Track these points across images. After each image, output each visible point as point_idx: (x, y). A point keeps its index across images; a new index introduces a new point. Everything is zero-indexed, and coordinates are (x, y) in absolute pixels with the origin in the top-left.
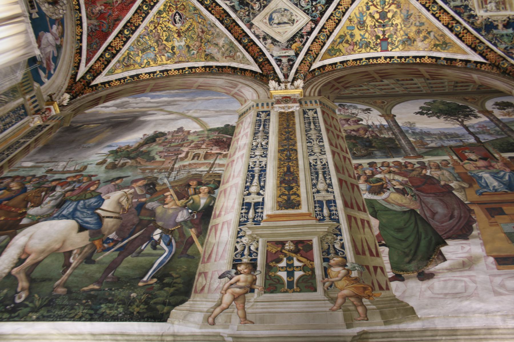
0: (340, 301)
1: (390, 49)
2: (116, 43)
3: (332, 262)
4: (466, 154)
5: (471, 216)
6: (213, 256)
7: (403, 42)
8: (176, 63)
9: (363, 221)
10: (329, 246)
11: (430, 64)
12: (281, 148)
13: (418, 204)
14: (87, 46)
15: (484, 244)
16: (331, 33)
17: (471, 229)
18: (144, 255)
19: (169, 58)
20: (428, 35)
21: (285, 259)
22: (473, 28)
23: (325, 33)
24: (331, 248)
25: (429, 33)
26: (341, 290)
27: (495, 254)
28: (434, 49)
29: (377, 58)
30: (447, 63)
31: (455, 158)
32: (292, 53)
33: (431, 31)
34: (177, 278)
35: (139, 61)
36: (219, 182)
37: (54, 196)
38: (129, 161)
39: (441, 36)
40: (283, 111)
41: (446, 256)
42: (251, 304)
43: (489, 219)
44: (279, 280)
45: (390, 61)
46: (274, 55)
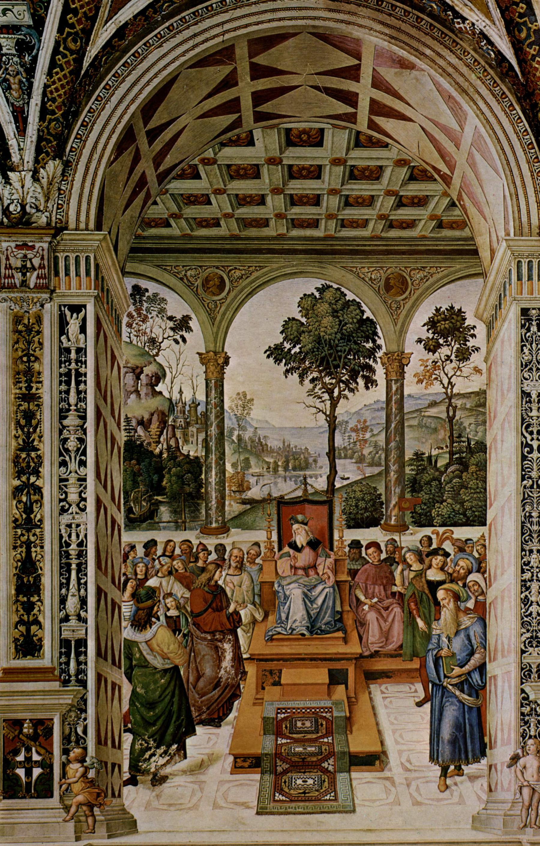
0: (73, 810)
3: (72, 755)
4: (295, 526)
9: (114, 684)
10: (71, 728)
13: (187, 657)
26: (77, 795)
31: (275, 537)
41: (188, 751)
43: (257, 693)
44: (18, 777)
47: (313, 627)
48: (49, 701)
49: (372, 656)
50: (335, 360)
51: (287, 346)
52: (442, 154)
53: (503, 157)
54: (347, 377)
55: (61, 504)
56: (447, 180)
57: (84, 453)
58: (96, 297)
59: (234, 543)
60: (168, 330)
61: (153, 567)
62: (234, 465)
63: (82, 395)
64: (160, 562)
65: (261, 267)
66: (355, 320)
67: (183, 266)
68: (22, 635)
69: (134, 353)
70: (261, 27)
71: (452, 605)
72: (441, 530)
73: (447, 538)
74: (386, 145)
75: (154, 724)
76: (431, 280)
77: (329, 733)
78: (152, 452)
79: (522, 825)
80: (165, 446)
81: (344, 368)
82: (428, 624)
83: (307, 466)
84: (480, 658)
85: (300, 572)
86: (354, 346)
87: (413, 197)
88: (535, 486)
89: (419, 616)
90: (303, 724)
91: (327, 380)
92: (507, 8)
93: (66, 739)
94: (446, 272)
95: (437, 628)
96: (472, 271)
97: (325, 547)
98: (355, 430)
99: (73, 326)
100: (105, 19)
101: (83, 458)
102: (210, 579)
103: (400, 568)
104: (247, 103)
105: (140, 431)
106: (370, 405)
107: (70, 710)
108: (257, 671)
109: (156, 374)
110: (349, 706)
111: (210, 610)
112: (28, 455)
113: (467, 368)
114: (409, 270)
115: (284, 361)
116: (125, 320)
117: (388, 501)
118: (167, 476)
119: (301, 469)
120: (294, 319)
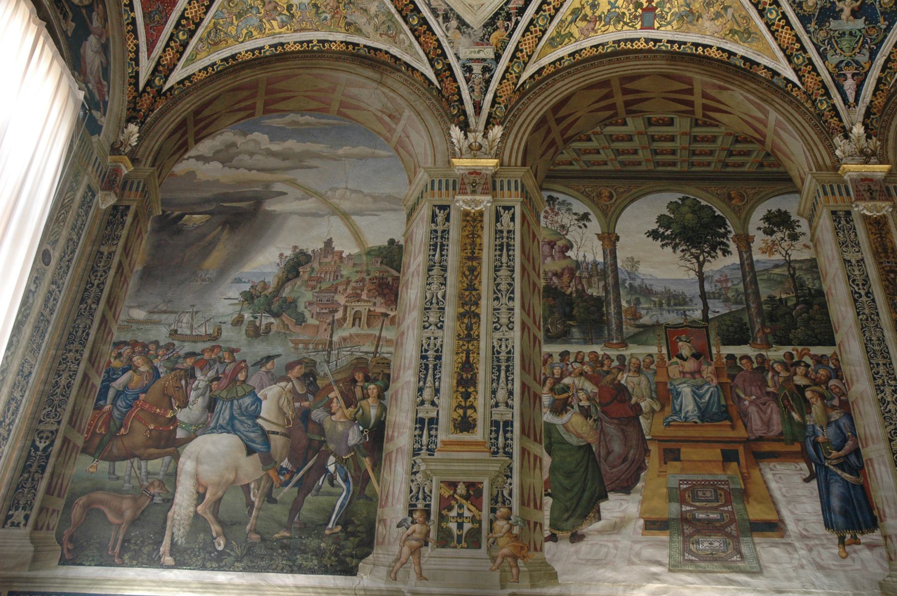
0: (499, 560)
1: (656, 25)
2: (193, 11)
3: (498, 513)
4: (680, 344)
6: (390, 498)
7: (681, 17)
8: (295, 31)
9: (536, 457)
11: (717, 60)
12: (461, 310)
13: (597, 436)
14: (144, 17)
15: (642, 502)
16: (557, 10)
17: (637, 480)
18: (324, 494)
19: (283, 24)
20: (723, 12)
21: (456, 506)
22: (797, 15)
23: (547, 13)
24: (500, 495)
25: (725, 8)
26: (502, 548)
27: (647, 516)
28: (728, 37)
29: (632, 40)
30: (744, 64)
31: (664, 351)
32: (488, 53)
33: (730, 7)
34: (359, 526)
35: (234, 33)
36: (388, 376)
37: (197, 388)
38: (272, 320)
39: (744, 18)
40: (469, 208)
41: (602, 515)
43: (661, 466)
44: (449, 532)
45: (654, 46)
47: (703, 416)
48: (480, 467)
51: (661, 230)
52: (756, 130)
56: (762, 143)
57: (513, 292)
59: (632, 354)
61: (567, 370)
63: (511, 258)
68: (460, 416)
71: (819, 403)
72: (800, 348)
73: (806, 354)
74: (717, 126)
77: (728, 502)
82: (802, 416)
83: (685, 303)
85: (688, 376)
87: (740, 151)
91: (693, 250)
93: (494, 500)
96: (790, 190)
97: (706, 358)
98: (719, 281)
99: (506, 217)
102: (615, 379)
103: (770, 374)
105: (555, 279)
107: (498, 476)
110: (743, 480)
113: (798, 244)
116: (543, 214)
117: (753, 329)
119: (681, 305)
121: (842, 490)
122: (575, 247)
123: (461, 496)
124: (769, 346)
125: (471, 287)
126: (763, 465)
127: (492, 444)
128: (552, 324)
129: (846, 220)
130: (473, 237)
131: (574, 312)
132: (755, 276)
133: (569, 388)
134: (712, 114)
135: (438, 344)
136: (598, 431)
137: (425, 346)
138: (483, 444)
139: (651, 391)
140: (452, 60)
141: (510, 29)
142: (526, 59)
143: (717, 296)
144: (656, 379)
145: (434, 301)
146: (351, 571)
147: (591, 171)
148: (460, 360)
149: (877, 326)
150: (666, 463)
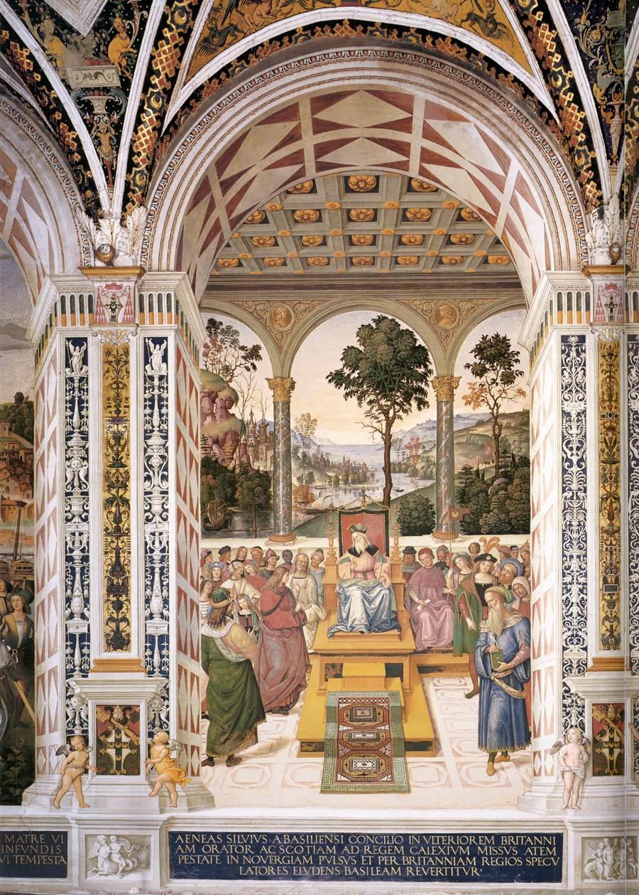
0: (157, 786)
3: (155, 737)
4: (355, 535)
5: (305, 676)
9: (193, 676)
12: (109, 496)
15: (300, 723)
17: (296, 701)
21: (114, 731)
31: (336, 544)
32: (110, 78)
34: (18, 755)
36: (32, 583)
42: (86, 787)
43: (321, 684)
44: (108, 757)
46: (73, 86)
47: (371, 625)
49: (424, 652)
50: (390, 383)
51: (347, 371)
53: (544, 199)
54: (401, 399)
55: (147, 514)
57: (166, 469)
58: (176, 331)
59: (299, 549)
60: (240, 359)
61: (228, 571)
62: (299, 479)
63: (164, 418)
64: (233, 566)
65: (325, 301)
66: (408, 348)
67: (253, 301)
69: (209, 379)
70: (322, 87)
71: (498, 606)
72: (488, 537)
75: (227, 712)
76: (478, 311)
78: (226, 468)
79: (564, 806)
80: (238, 462)
81: (398, 391)
82: (477, 623)
83: (364, 479)
84: (525, 655)
85: (360, 575)
86: (407, 371)
88: (575, 498)
89: (469, 616)
90: (362, 713)
91: (383, 402)
92: (544, 59)
94: (491, 304)
95: (485, 627)
96: (516, 302)
98: (409, 447)
100: (183, 80)
101: (165, 473)
102: (279, 582)
103: (450, 572)
104: (309, 156)
105: (215, 449)
106: (422, 424)
107: (154, 698)
108: (321, 664)
109: (230, 398)
111: (278, 609)
112: (117, 471)
113: (511, 390)
114: (457, 301)
115: (344, 385)
116: (202, 350)
117: (439, 511)
118: (239, 489)
119: (360, 482)
120: (352, 347)
121: (502, 705)
122: (241, 399)
123: (119, 721)
124: (453, 535)
125: (118, 463)
126: (426, 680)
127: (148, 663)
128: (212, 511)
129: (577, 350)
130: (118, 388)
131: (236, 496)
132: (452, 437)
133: (228, 592)
134: (433, 169)
135: (84, 542)
136: (258, 646)
137: (70, 545)
138: (137, 662)
139: (318, 595)
140: (60, 91)
141: (135, 32)
142: (169, 85)
143: (403, 468)
144: (324, 581)
145: (76, 483)
146: (17, 801)
147: (265, 276)
148: (109, 561)
149: (581, 506)
150: (327, 680)
